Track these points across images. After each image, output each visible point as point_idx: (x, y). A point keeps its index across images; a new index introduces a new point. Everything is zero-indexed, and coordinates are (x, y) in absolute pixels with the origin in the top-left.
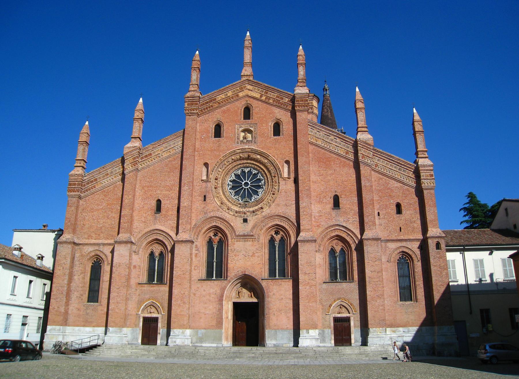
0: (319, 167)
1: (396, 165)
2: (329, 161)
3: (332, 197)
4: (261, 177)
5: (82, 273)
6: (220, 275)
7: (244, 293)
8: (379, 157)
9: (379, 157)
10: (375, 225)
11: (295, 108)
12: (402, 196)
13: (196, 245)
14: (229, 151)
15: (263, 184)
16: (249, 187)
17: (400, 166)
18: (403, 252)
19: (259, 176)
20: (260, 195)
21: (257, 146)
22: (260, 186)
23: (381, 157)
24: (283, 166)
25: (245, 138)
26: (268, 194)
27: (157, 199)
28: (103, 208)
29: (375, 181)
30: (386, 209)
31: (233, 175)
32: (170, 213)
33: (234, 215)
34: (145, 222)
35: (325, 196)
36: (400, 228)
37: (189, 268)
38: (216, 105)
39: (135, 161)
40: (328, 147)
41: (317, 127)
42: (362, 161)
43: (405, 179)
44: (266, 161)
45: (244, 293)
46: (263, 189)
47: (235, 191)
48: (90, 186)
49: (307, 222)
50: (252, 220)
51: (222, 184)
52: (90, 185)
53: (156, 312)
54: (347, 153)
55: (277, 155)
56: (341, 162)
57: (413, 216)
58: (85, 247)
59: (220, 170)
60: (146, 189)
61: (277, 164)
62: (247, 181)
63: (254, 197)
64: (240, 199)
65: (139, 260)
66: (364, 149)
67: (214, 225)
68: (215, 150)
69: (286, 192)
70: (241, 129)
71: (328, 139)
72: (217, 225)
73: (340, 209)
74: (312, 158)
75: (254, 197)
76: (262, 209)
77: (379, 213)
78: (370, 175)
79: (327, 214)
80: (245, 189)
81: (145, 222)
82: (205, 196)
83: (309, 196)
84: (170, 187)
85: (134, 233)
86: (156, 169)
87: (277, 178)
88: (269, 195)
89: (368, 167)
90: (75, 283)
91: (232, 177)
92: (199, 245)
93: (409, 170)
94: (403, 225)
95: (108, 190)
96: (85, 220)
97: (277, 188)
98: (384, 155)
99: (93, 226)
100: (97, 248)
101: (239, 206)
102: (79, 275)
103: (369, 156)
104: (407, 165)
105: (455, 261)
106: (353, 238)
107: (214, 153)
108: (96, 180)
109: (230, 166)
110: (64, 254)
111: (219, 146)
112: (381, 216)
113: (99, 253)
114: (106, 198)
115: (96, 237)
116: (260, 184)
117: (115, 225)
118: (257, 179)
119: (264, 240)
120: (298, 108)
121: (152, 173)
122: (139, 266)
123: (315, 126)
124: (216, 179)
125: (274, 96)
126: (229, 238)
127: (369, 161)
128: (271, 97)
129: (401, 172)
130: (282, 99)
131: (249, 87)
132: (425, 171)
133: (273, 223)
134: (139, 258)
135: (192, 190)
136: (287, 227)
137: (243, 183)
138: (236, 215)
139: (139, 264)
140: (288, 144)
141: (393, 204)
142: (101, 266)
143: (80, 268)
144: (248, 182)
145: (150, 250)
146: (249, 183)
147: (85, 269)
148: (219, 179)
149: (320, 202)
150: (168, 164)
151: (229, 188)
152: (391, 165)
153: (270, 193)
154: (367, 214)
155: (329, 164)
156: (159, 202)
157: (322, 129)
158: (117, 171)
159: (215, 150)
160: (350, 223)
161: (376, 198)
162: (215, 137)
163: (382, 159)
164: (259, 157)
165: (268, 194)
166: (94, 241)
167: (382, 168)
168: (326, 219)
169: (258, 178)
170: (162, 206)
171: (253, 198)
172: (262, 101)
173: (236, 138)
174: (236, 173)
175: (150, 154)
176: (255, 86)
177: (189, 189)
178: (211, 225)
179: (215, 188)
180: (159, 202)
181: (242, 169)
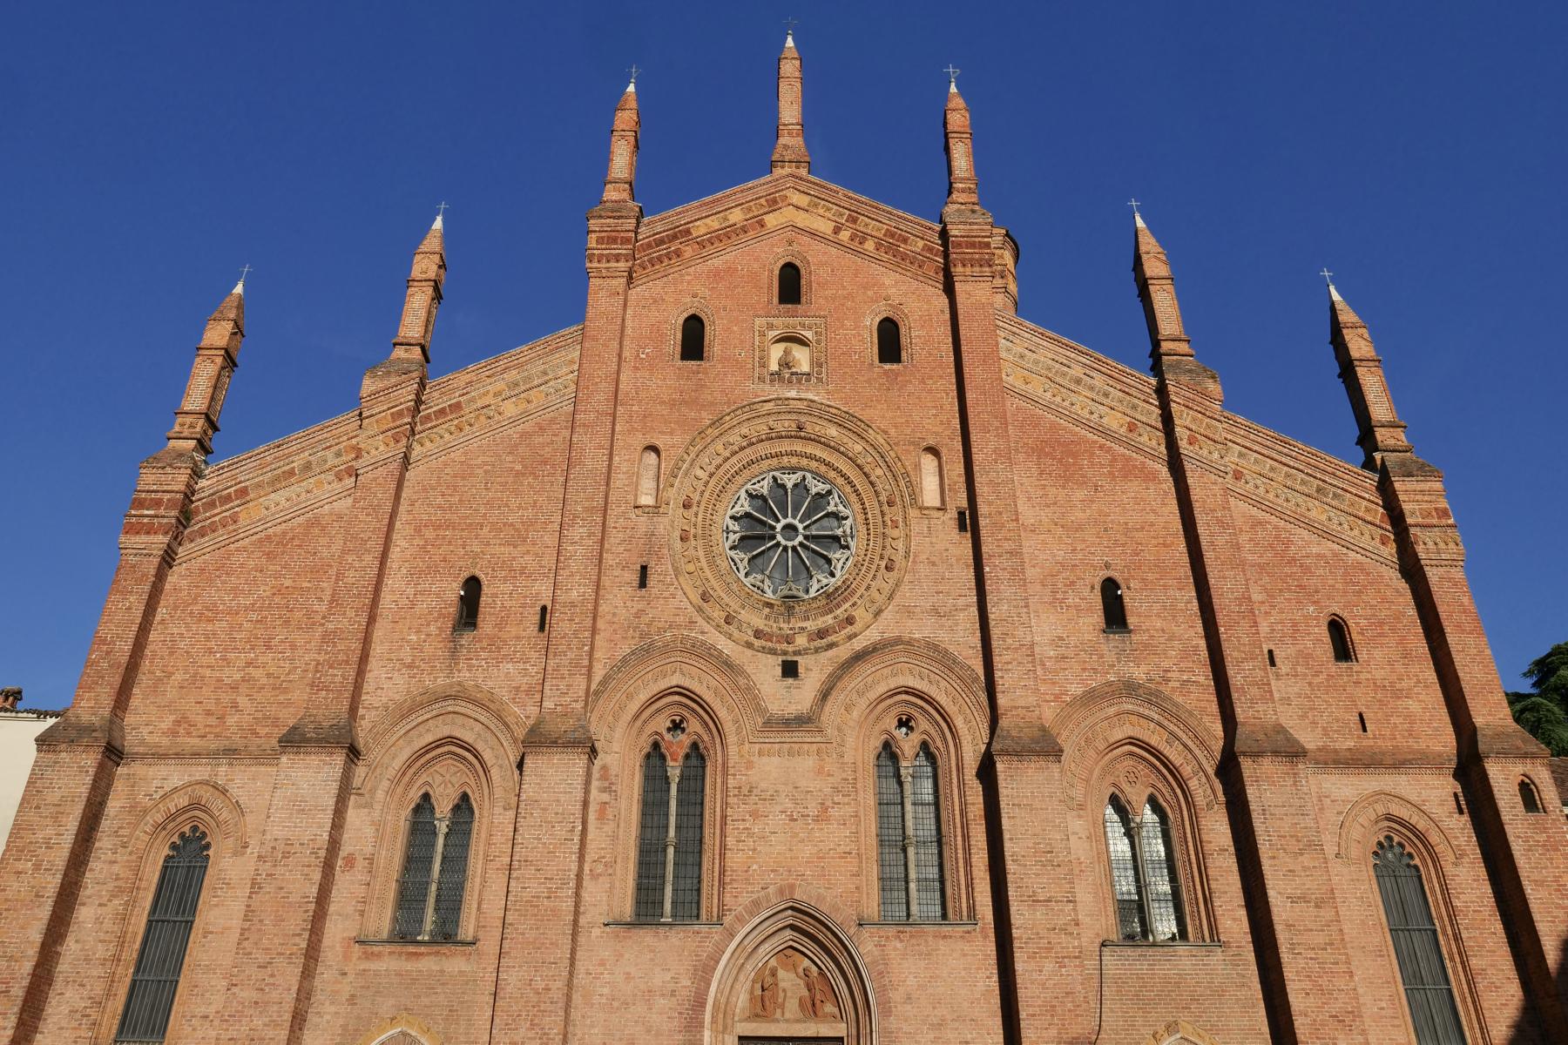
0: (1041, 474)
2: (1075, 455)
3: (1098, 588)
4: (841, 508)
7: (784, 990)
15: (848, 531)
16: (801, 544)
19: (832, 503)
20: (838, 573)
23: (1248, 445)
24: (918, 466)
25: (785, 363)
26: (869, 569)
27: (466, 575)
28: (253, 605)
31: (742, 497)
32: (514, 630)
33: (749, 645)
34: (410, 666)
35: (1073, 583)
38: (688, 251)
43: (1346, 526)
45: (784, 990)
46: (847, 553)
47: (750, 555)
49: (1021, 679)
50: (814, 671)
56: (1114, 460)
58: (152, 771)
63: (819, 581)
64: (766, 588)
67: (674, 683)
69: (934, 564)
70: (772, 334)
72: (687, 683)
74: (1017, 442)
75: (819, 581)
76: (851, 624)
80: (785, 549)
81: (410, 666)
82: (644, 568)
83: (1018, 575)
87: (898, 509)
88: (872, 572)
91: (739, 503)
93: (1356, 495)
96: (172, 654)
97: (900, 545)
98: (1259, 439)
109: (734, 459)
116: (839, 532)
117: (292, 677)
118: (828, 515)
119: (861, 749)
124: (686, 506)
126: (731, 739)
129: (1329, 500)
132: (1419, 497)
133: (893, 683)
136: (943, 700)
137: (779, 527)
138: (757, 643)
146: (800, 527)
149: (1057, 602)
151: (727, 545)
152: (1288, 475)
153: (874, 567)
154: (1235, 654)
164: (833, 431)
165: (869, 569)
166: (196, 741)
167: (1259, 482)
170: (482, 604)
171: (815, 586)
173: (757, 364)
178: (663, 684)
179: (682, 539)
181: (774, 477)
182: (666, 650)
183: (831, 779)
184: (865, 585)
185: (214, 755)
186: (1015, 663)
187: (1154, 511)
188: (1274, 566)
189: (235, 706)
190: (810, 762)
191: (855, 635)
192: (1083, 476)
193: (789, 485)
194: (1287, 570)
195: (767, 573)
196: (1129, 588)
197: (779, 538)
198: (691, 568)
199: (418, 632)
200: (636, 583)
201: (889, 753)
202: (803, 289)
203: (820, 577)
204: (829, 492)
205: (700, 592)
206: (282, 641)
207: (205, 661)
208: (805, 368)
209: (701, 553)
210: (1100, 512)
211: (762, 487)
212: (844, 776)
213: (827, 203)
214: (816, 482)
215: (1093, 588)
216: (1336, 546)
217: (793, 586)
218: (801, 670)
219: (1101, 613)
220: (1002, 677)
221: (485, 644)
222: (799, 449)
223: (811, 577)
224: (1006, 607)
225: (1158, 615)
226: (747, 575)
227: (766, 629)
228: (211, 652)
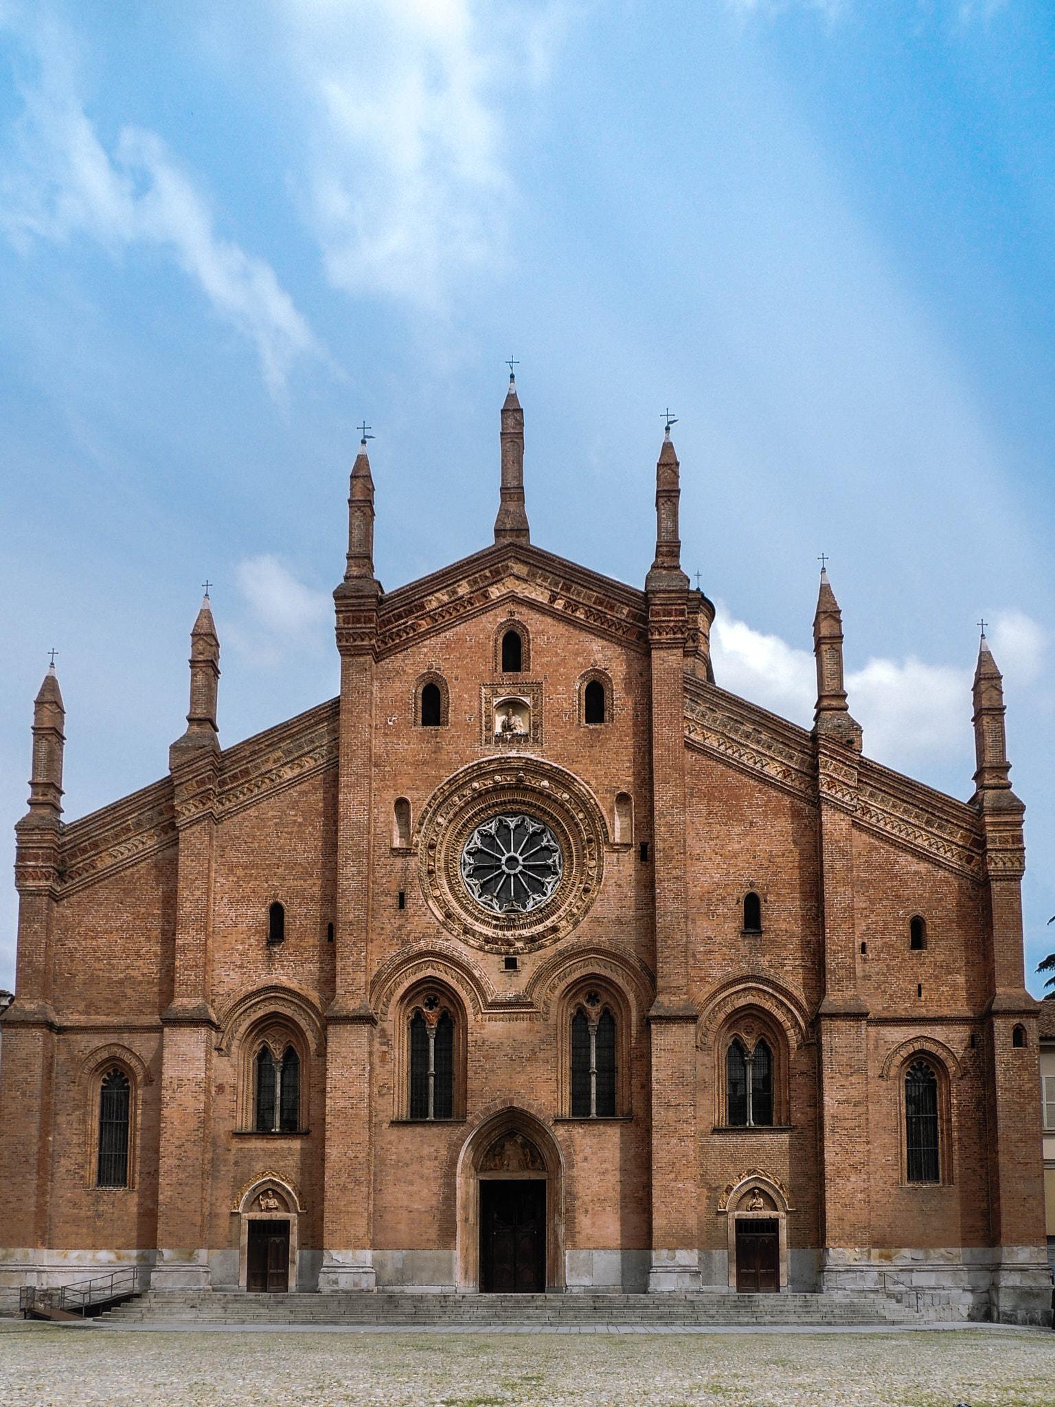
4: (552, 843)
5: (76, 1108)
8: (875, 787)
9: (875, 787)
10: (855, 979)
11: (650, 637)
12: (930, 899)
13: (383, 1030)
16: (521, 872)
17: (931, 813)
18: (922, 1051)
20: (549, 893)
25: (507, 727)
29: (860, 854)
31: (475, 837)
33: (481, 949)
34: (241, 967)
35: (724, 898)
36: (919, 986)
40: (736, 755)
42: (828, 797)
44: (566, 796)
47: (482, 881)
51: (446, 862)
55: (596, 778)
59: (440, 820)
61: (596, 804)
62: (514, 854)
63: (534, 899)
64: (495, 905)
65: (230, 1070)
70: (496, 701)
75: (534, 899)
78: (848, 839)
79: (727, 946)
81: (241, 967)
84: (304, 868)
85: (214, 997)
90: (59, 1134)
92: (390, 1031)
94: (926, 980)
101: (494, 922)
111: (438, 750)
114: (128, 900)
122: (234, 1087)
126: (470, 1011)
127: (848, 797)
128: (581, 600)
129: (933, 830)
134: (232, 1066)
135: (367, 877)
137: (504, 859)
139: (231, 1081)
141: (903, 919)
142: (128, 1087)
144: (517, 855)
145: (259, 1045)
146: (520, 859)
147: (86, 1095)
148: (438, 847)
153: (575, 889)
154: (833, 948)
155: (737, 805)
156: (277, 912)
161: (860, 903)
163: (884, 791)
165: (571, 891)
168: (724, 960)
171: (532, 903)
173: (484, 728)
175: (246, 772)
177: (360, 872)
181: (500, 820)
184: (568, 902)
188: (880, 881)
194: (889, 884)
195: (495, 894)
196: (765, 901)
197: (504, 868)
202: (524, 657)
204: (543, 831)
205: (445, 910)
211: (491, 828)
212: (548, 1032)
214: (532, 823)
215: (738, 902)
220: (662, 967)
221: (291, 950)
222: (519, 798)
223: (529, 896)
224: (669, 919)
225: (784, 920)
226: (480, 896)
227: (494, 936)
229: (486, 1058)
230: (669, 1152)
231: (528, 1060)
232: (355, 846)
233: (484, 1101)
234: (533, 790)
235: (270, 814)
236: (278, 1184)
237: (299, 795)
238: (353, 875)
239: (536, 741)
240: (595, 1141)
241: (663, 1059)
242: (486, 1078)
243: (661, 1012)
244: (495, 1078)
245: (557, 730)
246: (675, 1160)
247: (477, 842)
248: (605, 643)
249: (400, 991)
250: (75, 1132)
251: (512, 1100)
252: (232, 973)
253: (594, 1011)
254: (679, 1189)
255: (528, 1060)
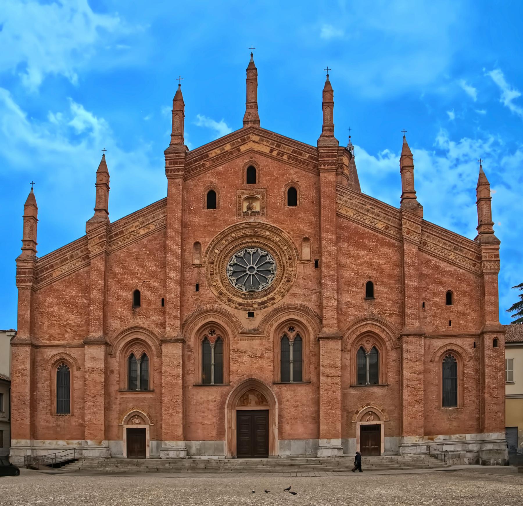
1: (452, 243)
2: (363, 238)
3: (365, 284)
4: (271, 260)
6: (219, 381)
13: (189, 345)
14: (229, 227)
15: (274, 268)
16: (256, 273)
20: (270, 283)
21: (266, 219)
22: (270, 271)
23: (431, 232)
25: (249, 208)
30: (434, 299)
33: (236, 308)
37: (181, 372)
39: (101, 240)
41: (349, 193)
44: (278, 239)
46: (273, 276)
47: (236, 278)
48: (45, 274)
49: (332, 315)
52: (44, 273)
53: (142, 422)
54: (387, 228)
55: (293, 231)
56: (378, 240)
57: (468, 306)
60: (119, 277)
61: (293, 242)
63: (262, 285)
64: (243, 289)
66: (410, 222)
68: (208, 225)
70: (244, 197)
71: (362, 208)
73: (374, 299)
75: (262, 285)
76: (273, 300)
77: (424, 303)
85: (108, 332)
86: (131, 251)
89: (414, 246)
91: (232, 260)
93: (468, 250)
95: (69, 279)
96: (42, 317)
99: (54, 324)
100: (61, 350)
101: (243, 296)
102: (43, 382)
103: (416, 231)
104: (466, 243)
105: (514, 360)
106: (389, 334)
107: (207, 229)
108: (52, 266)
110: (21, 358)
111: (215, 219)
112: (427, 308)
113: (64, 356)
115: (59, 337)
116: (270, 269)
118: (266, 263)
120: (322, 167)
121: (125, 257)
123: (345, 191)
125: (290, 150)
126: (231, 336)
130: (301, 154)
131: (256, 138)
134: (117, 362)
137: (247, 268)
138: (239, 307)
139: (117, 369)
140: (308, 217)
143: (44, 374)
144: (254, 266)
145: (130, 352)
146: (256, 267)
148: (215, 263)
150: (146, 245)
152: (444, 243)
156: (137, 294)
157: (354, 195)
158: (79, 256)
159: (208, 225)
160: (387, 316)
162: (208, 208)
164: (268, 233)
169: (267, 261)
171: (261, 287)
172: (272, 157)
173: (238, 209)
174: (238, 255)
175: (122, 232)
176: (263, 136)
180: (137, 294)
181: (245, 250)
182: (207, 311)
183: (265, 346)
185: (64, 346)
186: (330, 311)
187: (391, 258)
189: (67, 332)
190: (258, 342)
191: (275, 303)
192: (365, 246)
193: (252, 253)
195: (243, 284)
197: (248, 272)
198: (215, 284)
199: (121, 308)
200: (195, 290)
201: (285, 339)
203: (263, 284)
204: (267, 255)
206: (76, 312)
207: (54, 319)
208: (258, 209)
209: (218, 279)
210: (370, 259)
211: (241, 254)
212: (269, 345)
213: (267, 139)
216: (456, 268)
217: (253, 288)
218: (255, 315)
219: (365, 293)
221: (144, 311)
223: (260, 284)
227: (243, 302)
228: (54, 316)
229: (239, 357)
230: (328, 397)
231: (260, 357)
232: (174, 264)
233: (238, 376)
234: (262, 237)
235: (134, 250)
236: (140, 413)
237: (148, 241)
238: (174, 277)
239: (263, 214)
240: (292, 393)
241: (325, 356)
242: (239, 366)
243: (324, 335)
244: (244, 365)
245: (273, 209)
246: (331, 401)
247: (234, 260)
248: (297, 170)
249: (197, 328)
250: (45, 390)
251: (252, 375)
252: (116, 321)
253: (292, 335)
254: (333, 413)
255: (260, 357)
